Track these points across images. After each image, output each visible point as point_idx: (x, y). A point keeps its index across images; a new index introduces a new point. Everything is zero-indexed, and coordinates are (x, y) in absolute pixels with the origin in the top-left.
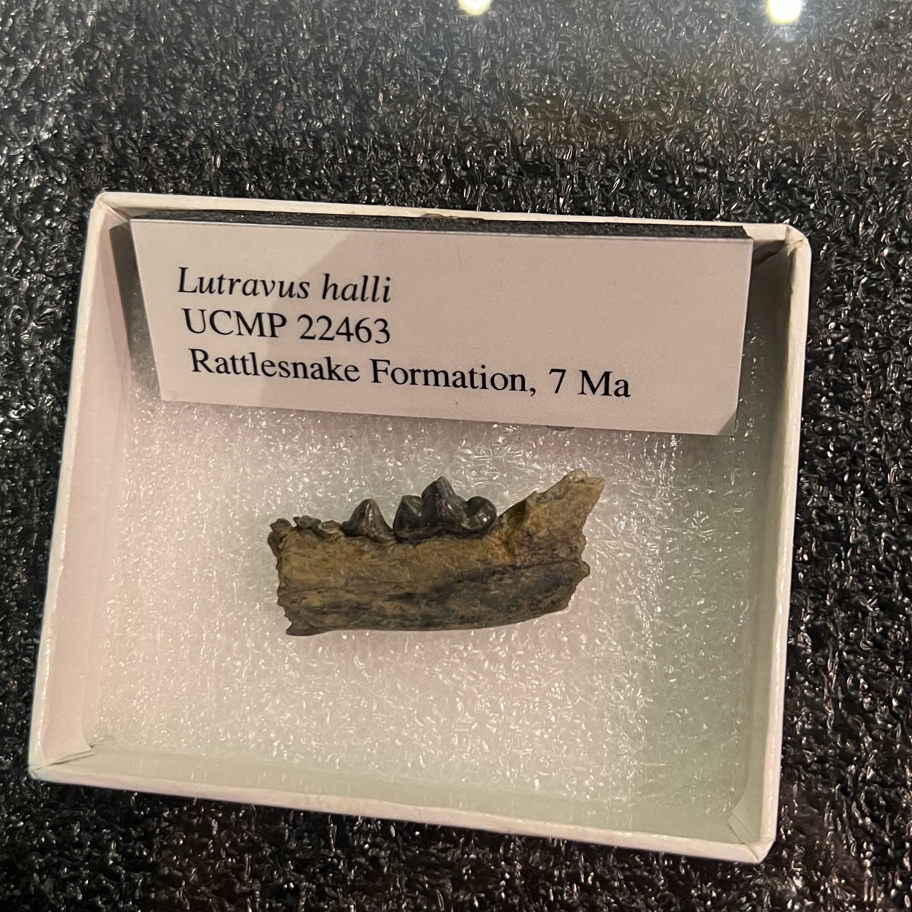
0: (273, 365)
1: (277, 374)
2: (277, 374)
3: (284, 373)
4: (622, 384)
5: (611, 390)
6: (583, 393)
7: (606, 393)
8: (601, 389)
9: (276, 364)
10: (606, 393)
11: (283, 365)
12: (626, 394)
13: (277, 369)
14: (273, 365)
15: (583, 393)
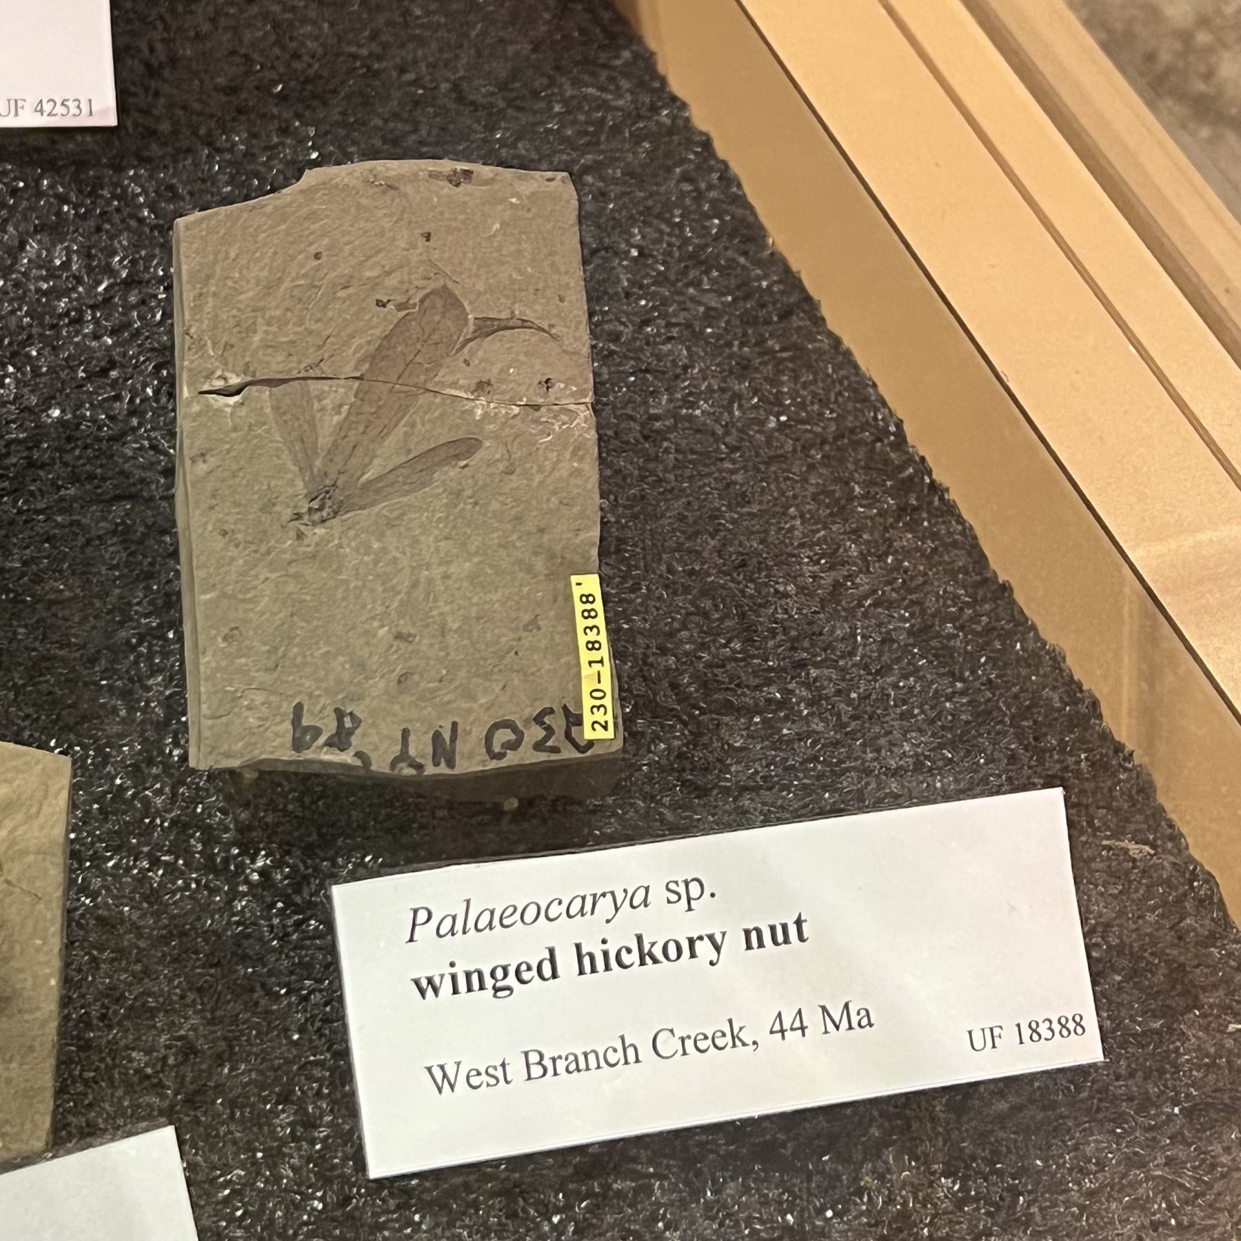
0: (479, 1074)
1: (485, 1085)
2: (485, 1085)
3: (493, 1081)
4: (863, 1013)
5: (855, 1024)
6: (826, 1032)
7: (850, 1028)
8: (845, 1024)
9: (483, 1071)
10: (850, 1028)
11: (491, 1071)
12: (870, 1025)
13: (484, 1078)
14: (479, 1074)
15: (826, 1032)
